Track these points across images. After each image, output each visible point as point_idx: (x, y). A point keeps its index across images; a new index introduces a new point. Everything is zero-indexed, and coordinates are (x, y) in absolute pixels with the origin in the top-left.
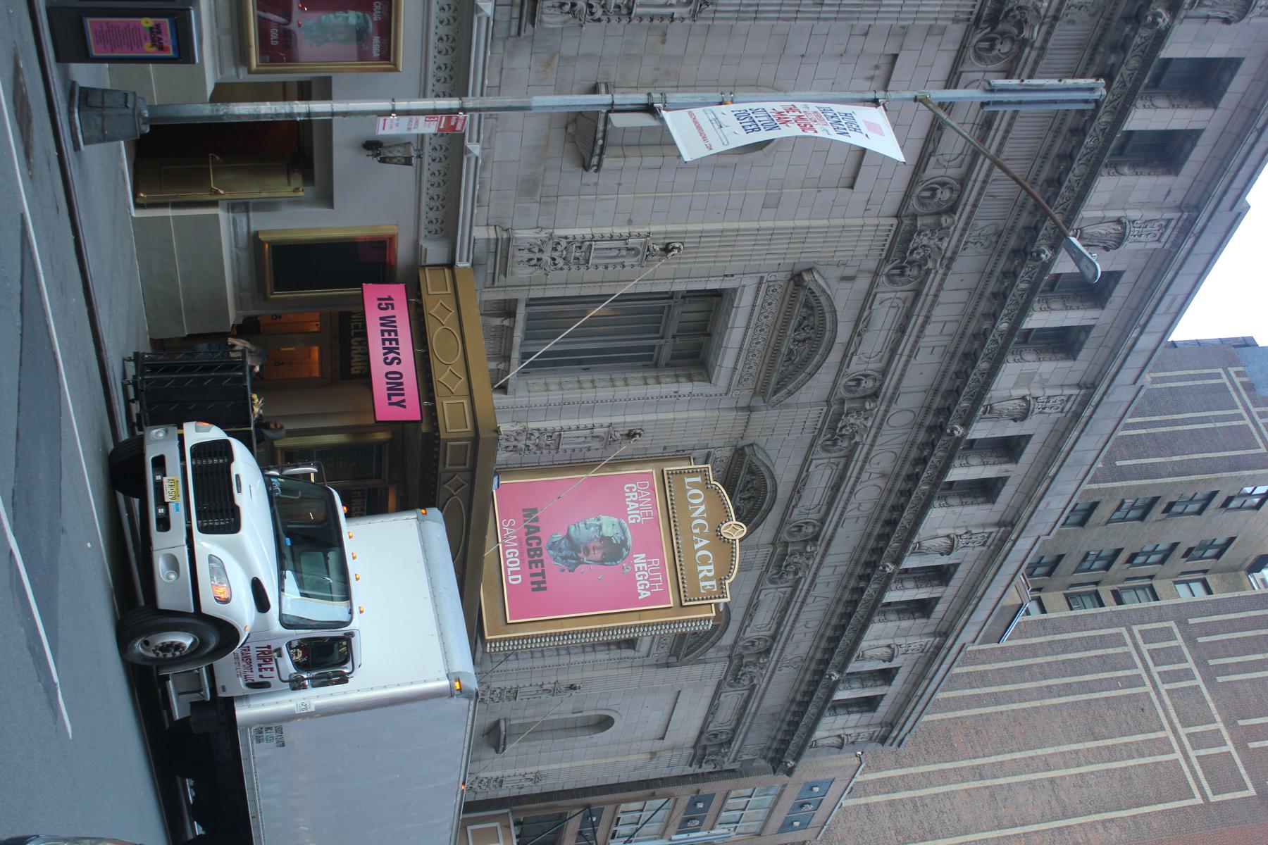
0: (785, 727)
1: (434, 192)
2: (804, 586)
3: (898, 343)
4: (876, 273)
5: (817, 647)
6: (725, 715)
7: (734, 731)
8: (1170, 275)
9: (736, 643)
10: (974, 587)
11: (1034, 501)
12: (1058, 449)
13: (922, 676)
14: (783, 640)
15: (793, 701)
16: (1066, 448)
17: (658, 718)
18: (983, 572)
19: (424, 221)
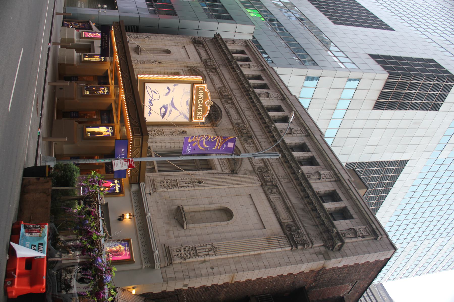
0: (313, 213)
1: (142, 240)
2: (256, 141)
3: (222, 82)
4: (206, 71)
5: (285, 168)
6: (284, 215)
7: (294, 221)
8: (268, 72)
9: (253, 168)
10: (319, 149)
11: (300, 118)
12: (290, 106)
13: (347, 191)
14: (269, 165)
15: (302, 198)
16: (291, 104)
17: (251, 211)
18: (315, 143)
19: (141, 251)
